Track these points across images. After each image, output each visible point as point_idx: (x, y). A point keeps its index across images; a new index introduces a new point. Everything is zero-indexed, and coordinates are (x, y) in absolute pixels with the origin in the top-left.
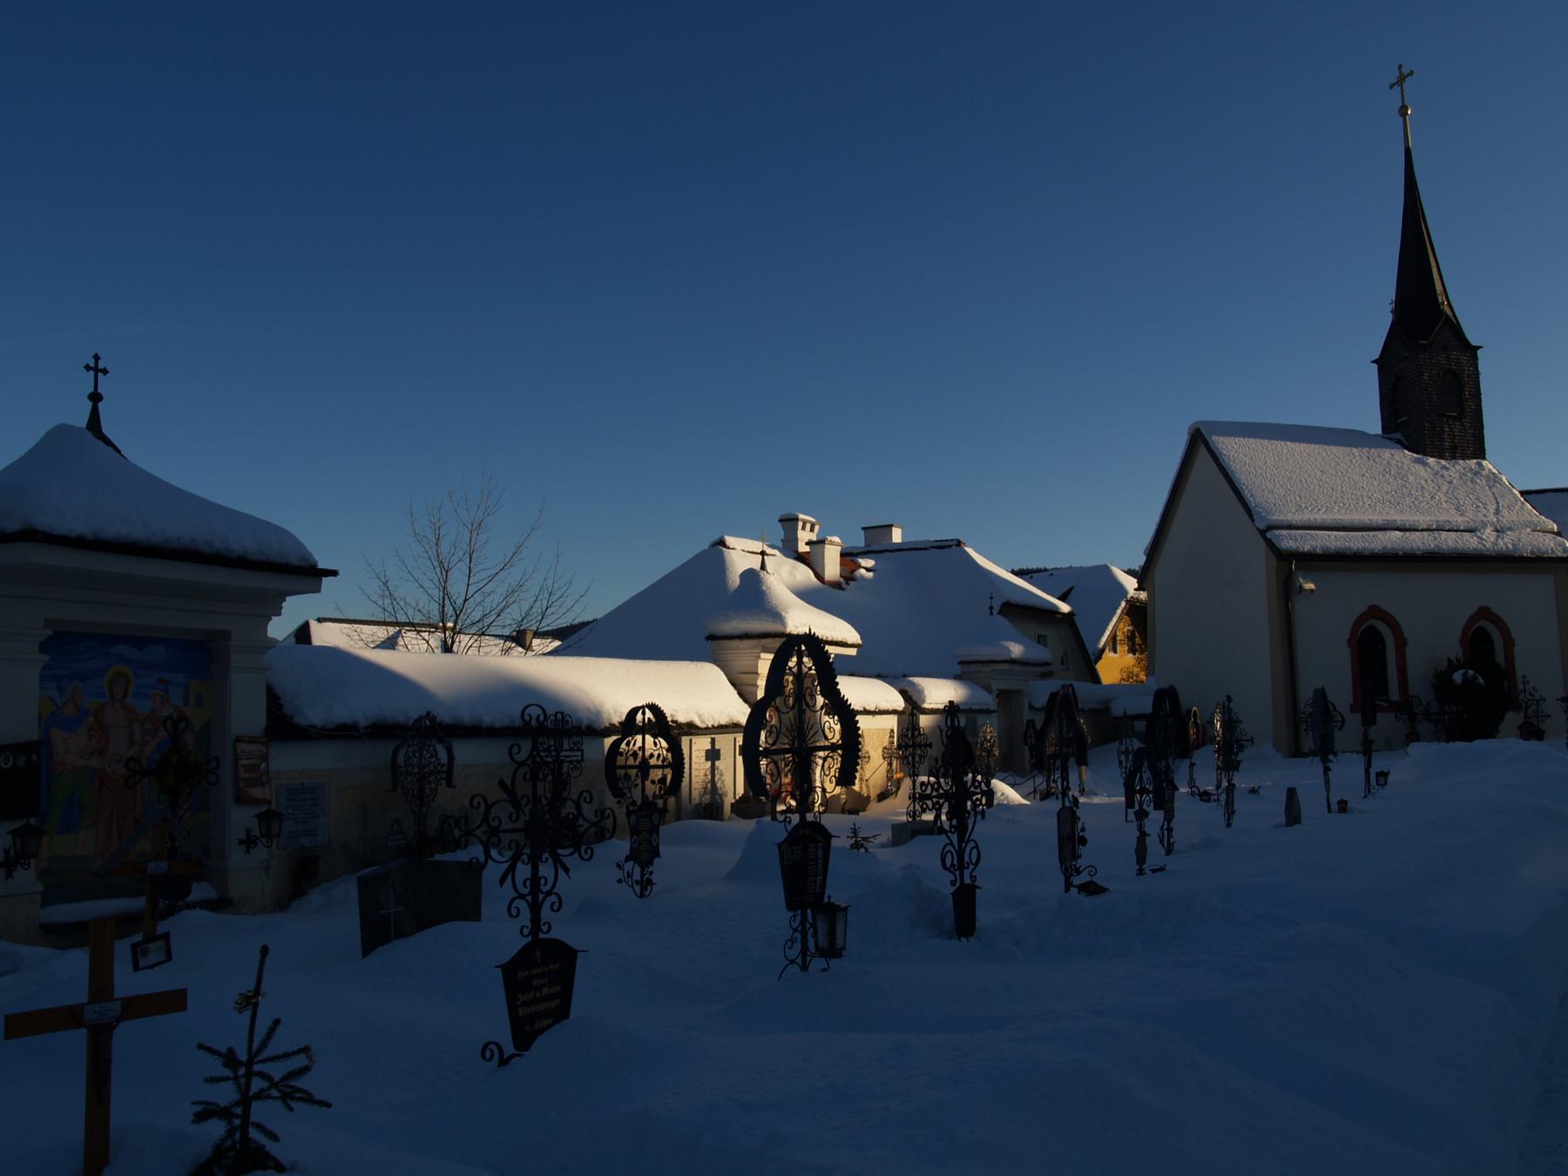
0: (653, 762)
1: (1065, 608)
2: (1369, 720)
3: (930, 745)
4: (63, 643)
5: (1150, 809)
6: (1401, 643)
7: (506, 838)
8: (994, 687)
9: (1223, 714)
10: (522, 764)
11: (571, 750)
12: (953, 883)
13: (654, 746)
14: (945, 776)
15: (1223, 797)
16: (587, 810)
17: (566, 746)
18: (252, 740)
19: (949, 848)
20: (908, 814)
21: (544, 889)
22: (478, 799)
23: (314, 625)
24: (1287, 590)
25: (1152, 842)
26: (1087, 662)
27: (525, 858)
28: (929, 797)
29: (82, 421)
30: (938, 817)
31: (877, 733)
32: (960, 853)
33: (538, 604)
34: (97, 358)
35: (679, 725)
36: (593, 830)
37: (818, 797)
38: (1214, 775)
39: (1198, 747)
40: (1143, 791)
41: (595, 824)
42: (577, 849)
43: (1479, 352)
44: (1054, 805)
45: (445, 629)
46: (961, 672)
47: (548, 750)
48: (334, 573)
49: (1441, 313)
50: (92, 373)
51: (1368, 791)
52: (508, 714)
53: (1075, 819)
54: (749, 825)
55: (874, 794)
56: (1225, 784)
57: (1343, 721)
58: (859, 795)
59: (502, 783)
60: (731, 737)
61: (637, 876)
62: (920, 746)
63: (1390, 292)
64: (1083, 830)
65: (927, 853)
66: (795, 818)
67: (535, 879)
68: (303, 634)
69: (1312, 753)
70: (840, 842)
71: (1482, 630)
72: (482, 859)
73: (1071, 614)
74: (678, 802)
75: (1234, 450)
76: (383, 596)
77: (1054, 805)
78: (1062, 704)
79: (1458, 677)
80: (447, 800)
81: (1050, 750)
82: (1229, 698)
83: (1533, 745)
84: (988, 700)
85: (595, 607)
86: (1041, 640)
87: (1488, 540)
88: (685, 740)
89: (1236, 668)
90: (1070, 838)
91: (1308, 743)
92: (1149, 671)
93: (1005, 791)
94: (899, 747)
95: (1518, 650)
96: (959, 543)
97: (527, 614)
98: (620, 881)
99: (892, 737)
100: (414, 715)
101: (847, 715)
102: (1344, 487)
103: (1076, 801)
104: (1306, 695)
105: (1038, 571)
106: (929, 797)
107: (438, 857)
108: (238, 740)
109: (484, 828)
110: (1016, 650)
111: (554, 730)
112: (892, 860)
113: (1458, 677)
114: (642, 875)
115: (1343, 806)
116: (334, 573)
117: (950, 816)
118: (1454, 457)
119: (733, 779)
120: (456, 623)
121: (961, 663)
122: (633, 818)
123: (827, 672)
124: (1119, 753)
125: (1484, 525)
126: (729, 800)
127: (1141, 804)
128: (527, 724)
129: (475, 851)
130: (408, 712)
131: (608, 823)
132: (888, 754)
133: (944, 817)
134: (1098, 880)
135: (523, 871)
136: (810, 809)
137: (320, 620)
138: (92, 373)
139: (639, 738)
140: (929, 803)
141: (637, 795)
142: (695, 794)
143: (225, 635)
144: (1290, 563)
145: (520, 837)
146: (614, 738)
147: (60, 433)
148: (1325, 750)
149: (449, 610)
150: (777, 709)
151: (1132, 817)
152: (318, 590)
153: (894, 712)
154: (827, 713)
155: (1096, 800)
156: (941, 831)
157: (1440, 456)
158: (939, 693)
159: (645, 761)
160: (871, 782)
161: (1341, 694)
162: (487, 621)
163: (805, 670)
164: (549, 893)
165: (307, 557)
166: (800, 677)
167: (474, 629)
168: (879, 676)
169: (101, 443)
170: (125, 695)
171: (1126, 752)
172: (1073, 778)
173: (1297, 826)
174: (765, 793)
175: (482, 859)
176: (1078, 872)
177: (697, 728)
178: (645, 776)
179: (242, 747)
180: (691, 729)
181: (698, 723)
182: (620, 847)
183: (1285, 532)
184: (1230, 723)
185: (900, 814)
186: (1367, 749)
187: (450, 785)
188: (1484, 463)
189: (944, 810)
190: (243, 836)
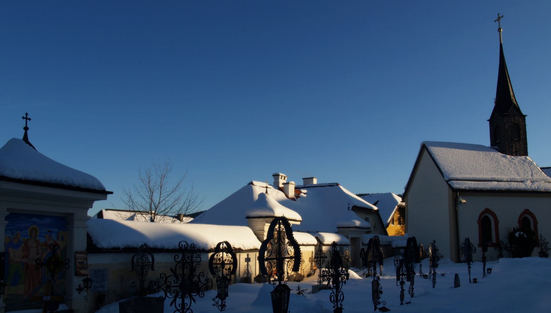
0: (226, 262)
1: (375, 208)
2: (485, 250)
3: (326, 257)
4: (13, 217)
5: (405, 281)
6: (497, 222)
7: (173, 289)
8: (349, 236)
9: (432, 247)
10: (179, 262)
11: (197, 257)
12: (334, 307)
13: (227, 257)
14: (331, 268)
15: (432, 277)
16: (202, 279)
17: (195, 256)
18: (81, 253)
19: (333, 294)
20: (318, 282)
21: (186, 308)
22: (163, 275)
23: (104, 212)
24: (456, 202)
25: (406, 293)
26: (383, 228)
27: (179, 296)
28: (326, 276)
29: (21, 137)
30: (329, 283)
31: (307, 253)
32: (337, 296)
33: (185, 205)
34: (27, 114)
35: (236, 249)
36: (204, 286)
37: (286, 275)
38: (428, 269)
39: (423, 259)
40: (403, 275)
41: (205, 284)
42: (198, 293)
43: (526, 118)
44: (371, 279)
45: (151, 213)
46: (338, 231)
47: (188, 257)
48: (112, 193)
49: (513, 103)
50: (25, 120)
51: (484, 275)
52: (174, 244)
53: (378, 284)
54: (260, 285)
55: (306, 274)
56: (432, 272)
57: (475, 250)
58: (300, 275)
59: (171, 269)
60: (254, 253)
61: (220, 303)
62: (323, 257)
63: (494, 95)
64: (381, 288)
65: (325, 296)
66: (277, 283)
67: (183, 304)
68: (100, 215)
69: (464, 262)
70: (293, 292)
71: (526, 218)
72: (164, 297)
73: (377, 211)
74: (235, 276)
75: (436, 151)
76: (129, 201)
77: (371, 279)
78: (374, 243)
79: (517, 234)
80: (151, 275)
81: (369, 259)
82: (434, 241)
83: (544, 259)
84: (347, 241)
85: (206, 206)
86: (367, 219)
87: (528, 185)
88: (238, 255)
89: (437, 229)
90: (376, 291)
91: (463, 258)
92: (406, 231)
93: (353, 274)
94: (315, 258)
95: (539, 225)
96: (337, 184)
97: (181, 208)
98: (214, 305)
99: (312, 254)
100: (140, 244)
101: (296, 246)
102: (477, 166)
103: (379, 278)
104: (462, 240)
105: (366, 195)
106: (326, 276)
107: (148, 296)
108: (76, 253)
109: (165, 285)
110: (358, 223)
111: (190, 250)
112: (313, 298)
113: (517, 234)
114: (222, 303)
115: (475, 281)
116: (112, 193)
117: (333, 283)
118: (516, 155)
119: (255, 269)
120: (155, 211)
121: (338, 228)
122: (219, 282)
123: (289, 230)
124: (395, 261)
125: (527, 180)
126: (253, 276)
127: (402, 279)
128: (181, 248)
129: (162, 294)
130: (138, 243)
131: (210, 284)
132: (311, 260)
133: (331, 283)
134: (386, 306)
135: (179, 301)
136: (283, 280)
137: (106, 210)
138: (25, 120)
139: (221, 253)
140: (326, 278)
141: (220, 274)
142: (241, 274)
143: (72, 215)
144: (457, 193)
145: (178, 289)
146: (212, 253)
147: (13, 141)
148: (469, 261)
149: (153, 206)
150: (271, 244)
151: (399, 284)
152: (105, 199)
153: (313, 245)
154: (289, 245)
155: (386, 278)
156: (330, 288)
157: (512, 155)
158: (330, 238)
159: (223, 262)
160: (305, 270)
161: (475, 240)
162: (167, 211)
163: (281, 229)
164: (188, 309)
165: (102, 186)
166: (279, 232)
167: (162, 214)
168: (308, 232)
169: (28, 145)
170: (36, 236)
171: (397, 261)
172: (378, 269)
173: (458, 288)
174: (266, 274)
175: (164, 297)
176: (379, 303)
177: (242, 250)
178: (223, 267)
179: (77, 255)
180: (240, 250)
181: (243, 248)
182: (214, 293)
183: (455, 182)
184: (435, 250)
185: (315, 282)
186: (484, 260)
187: (153, 270)
188: (527, 157)
189: (331, 280)
190: (78, 287)
